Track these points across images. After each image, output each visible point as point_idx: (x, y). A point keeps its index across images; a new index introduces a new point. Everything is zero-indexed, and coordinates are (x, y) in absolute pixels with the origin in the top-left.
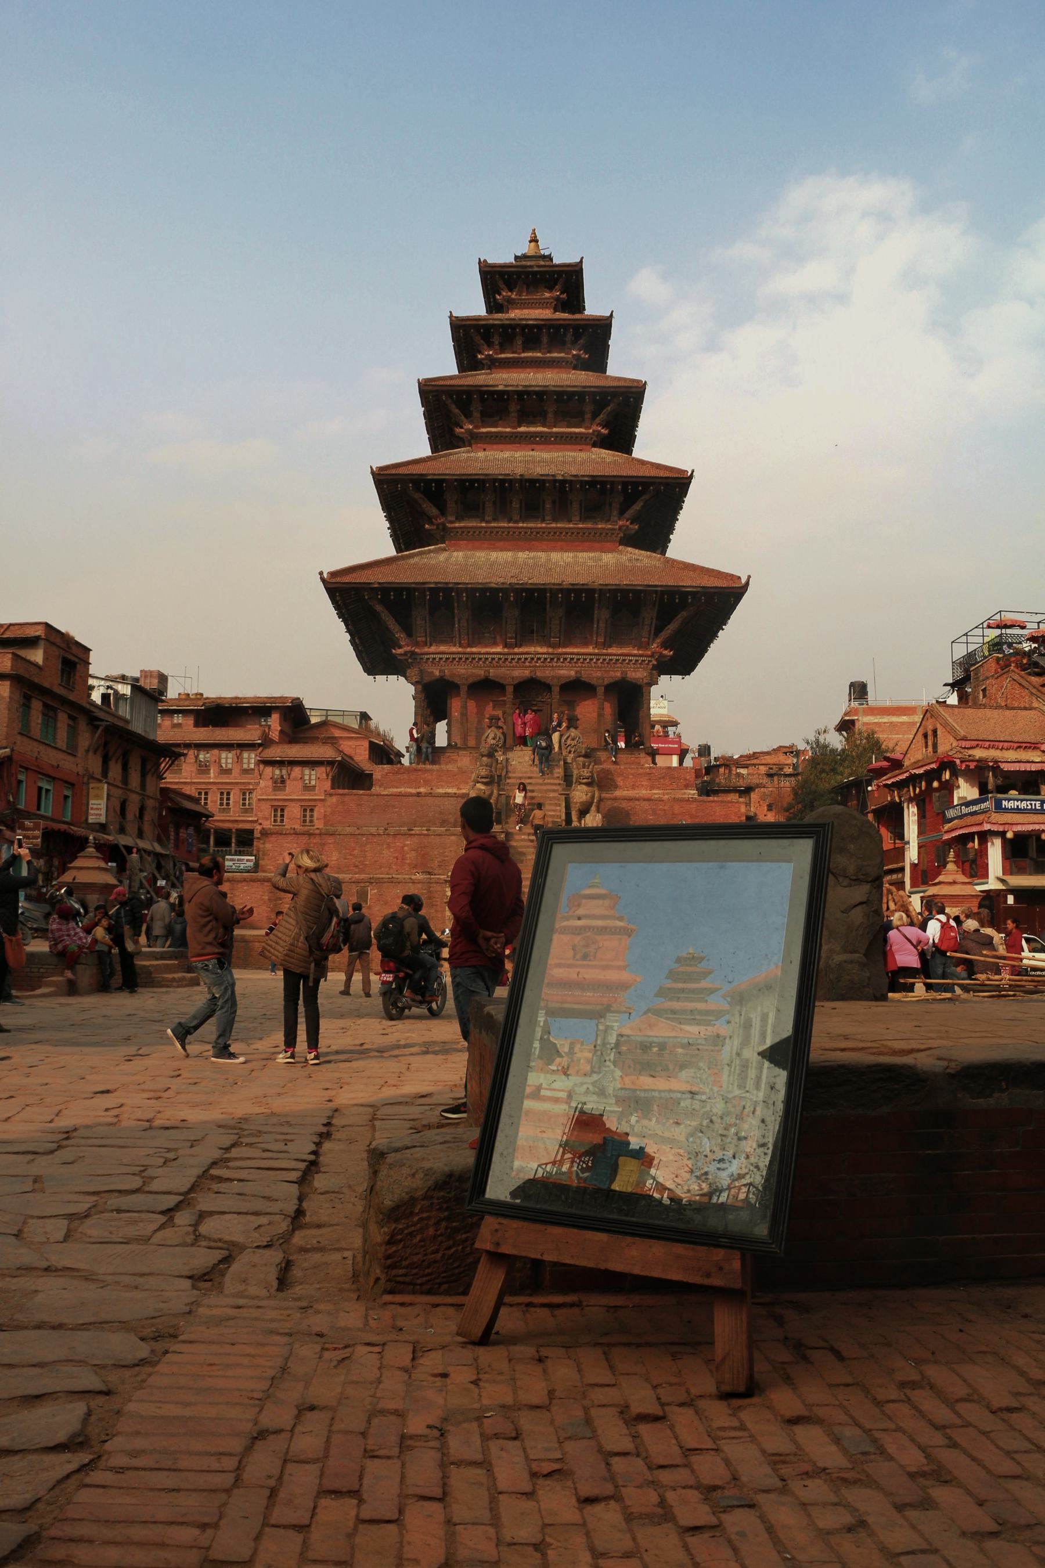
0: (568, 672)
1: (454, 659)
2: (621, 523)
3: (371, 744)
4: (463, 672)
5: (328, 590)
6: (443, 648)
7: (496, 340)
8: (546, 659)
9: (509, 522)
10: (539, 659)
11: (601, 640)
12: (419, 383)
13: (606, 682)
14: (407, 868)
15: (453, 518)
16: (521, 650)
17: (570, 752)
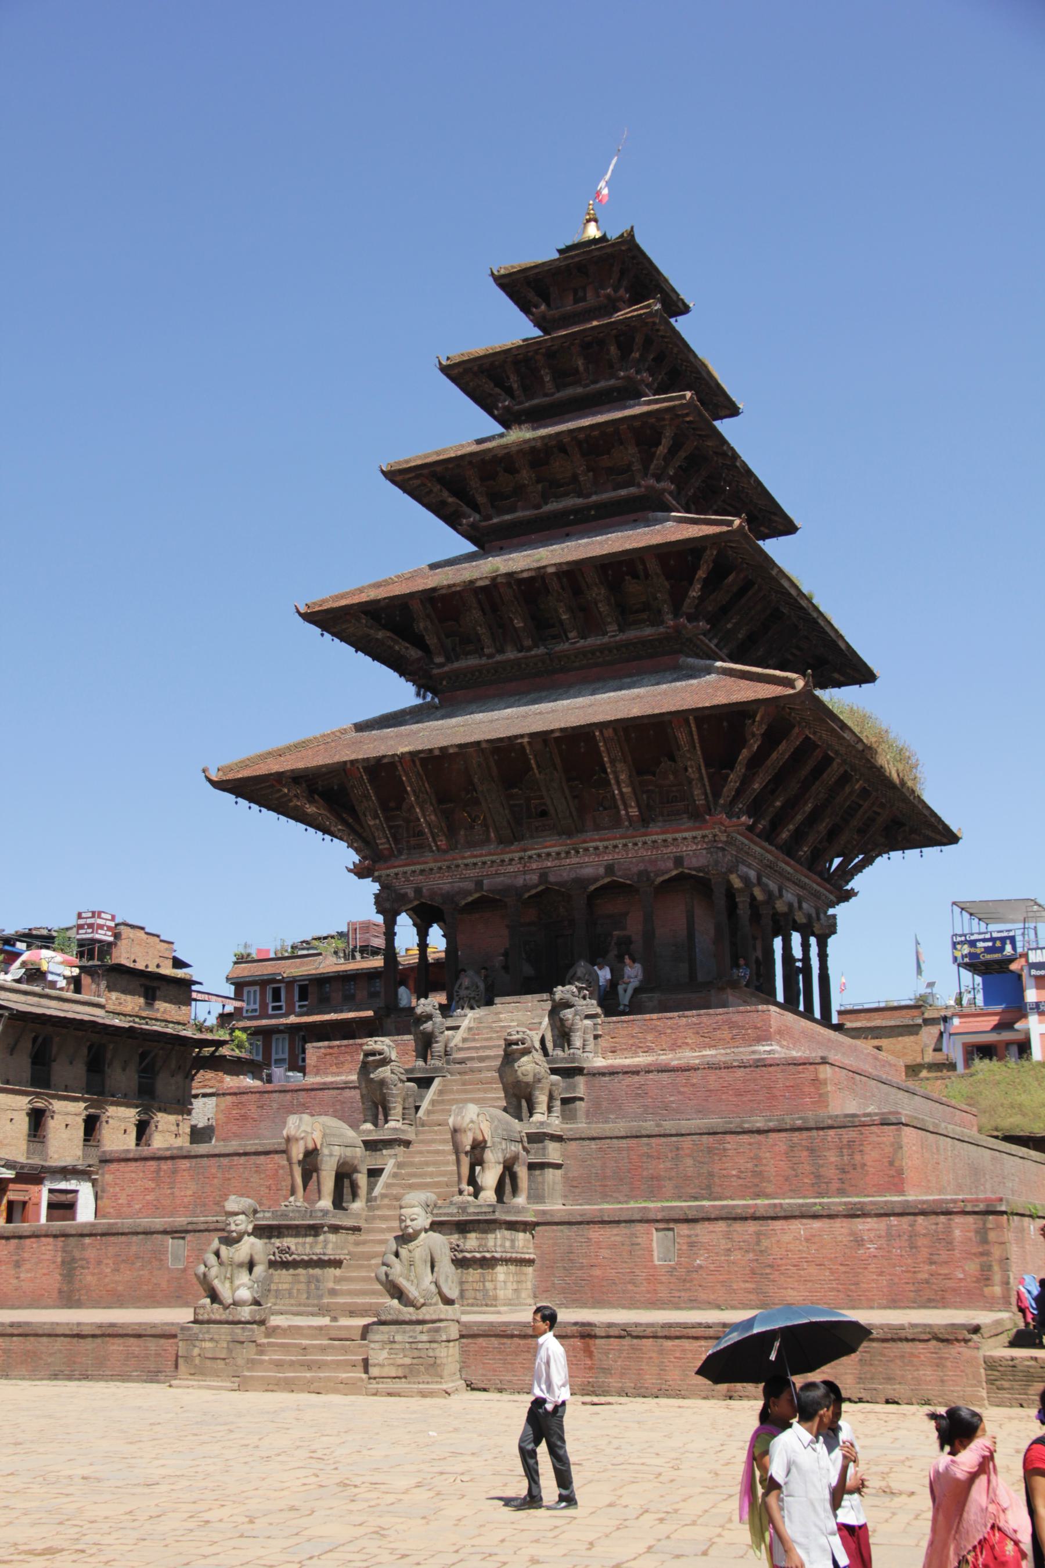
1: (431, 870)
8: (558, 854)
9: (520, 651)
10: (549, 854)
11: (634, 812)
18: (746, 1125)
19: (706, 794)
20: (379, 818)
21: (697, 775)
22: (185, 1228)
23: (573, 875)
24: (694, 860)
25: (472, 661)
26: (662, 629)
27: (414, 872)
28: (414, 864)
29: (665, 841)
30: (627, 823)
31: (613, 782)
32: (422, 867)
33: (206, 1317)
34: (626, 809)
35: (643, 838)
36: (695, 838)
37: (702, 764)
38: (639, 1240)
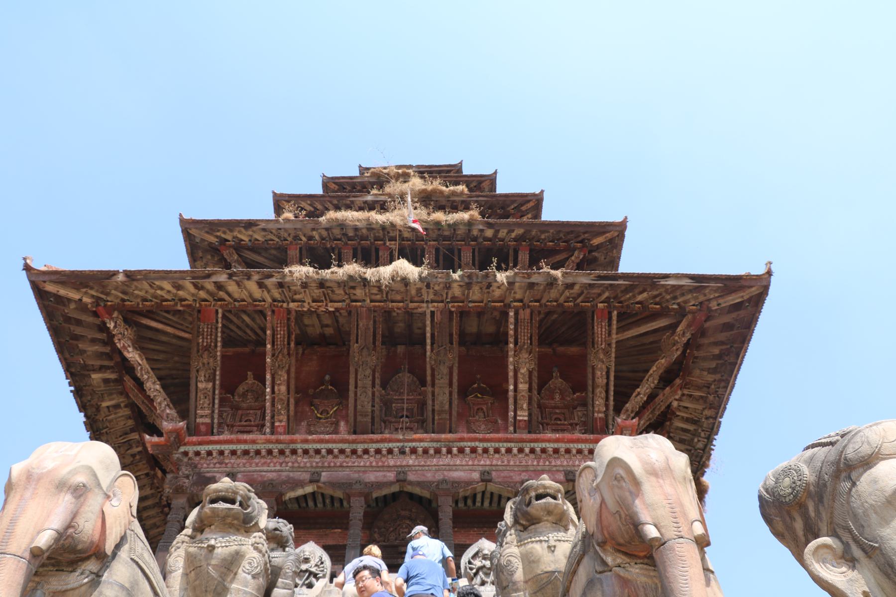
1: (258, 452)
5: (40, 294)
8: (426, 451)
10: (414, 451)
11: (523, 416)
12: (275, 194)
19: (607, 406)
21: (605, 381)
23: (439, 476)
27: (233, 453)
28: (239, 442)
29: (556, 451)
30: (511, 429)
31: (511, 374)
32: (246, 447)
34: (515, 411)
35: (532, 445)
37: (613, 369)
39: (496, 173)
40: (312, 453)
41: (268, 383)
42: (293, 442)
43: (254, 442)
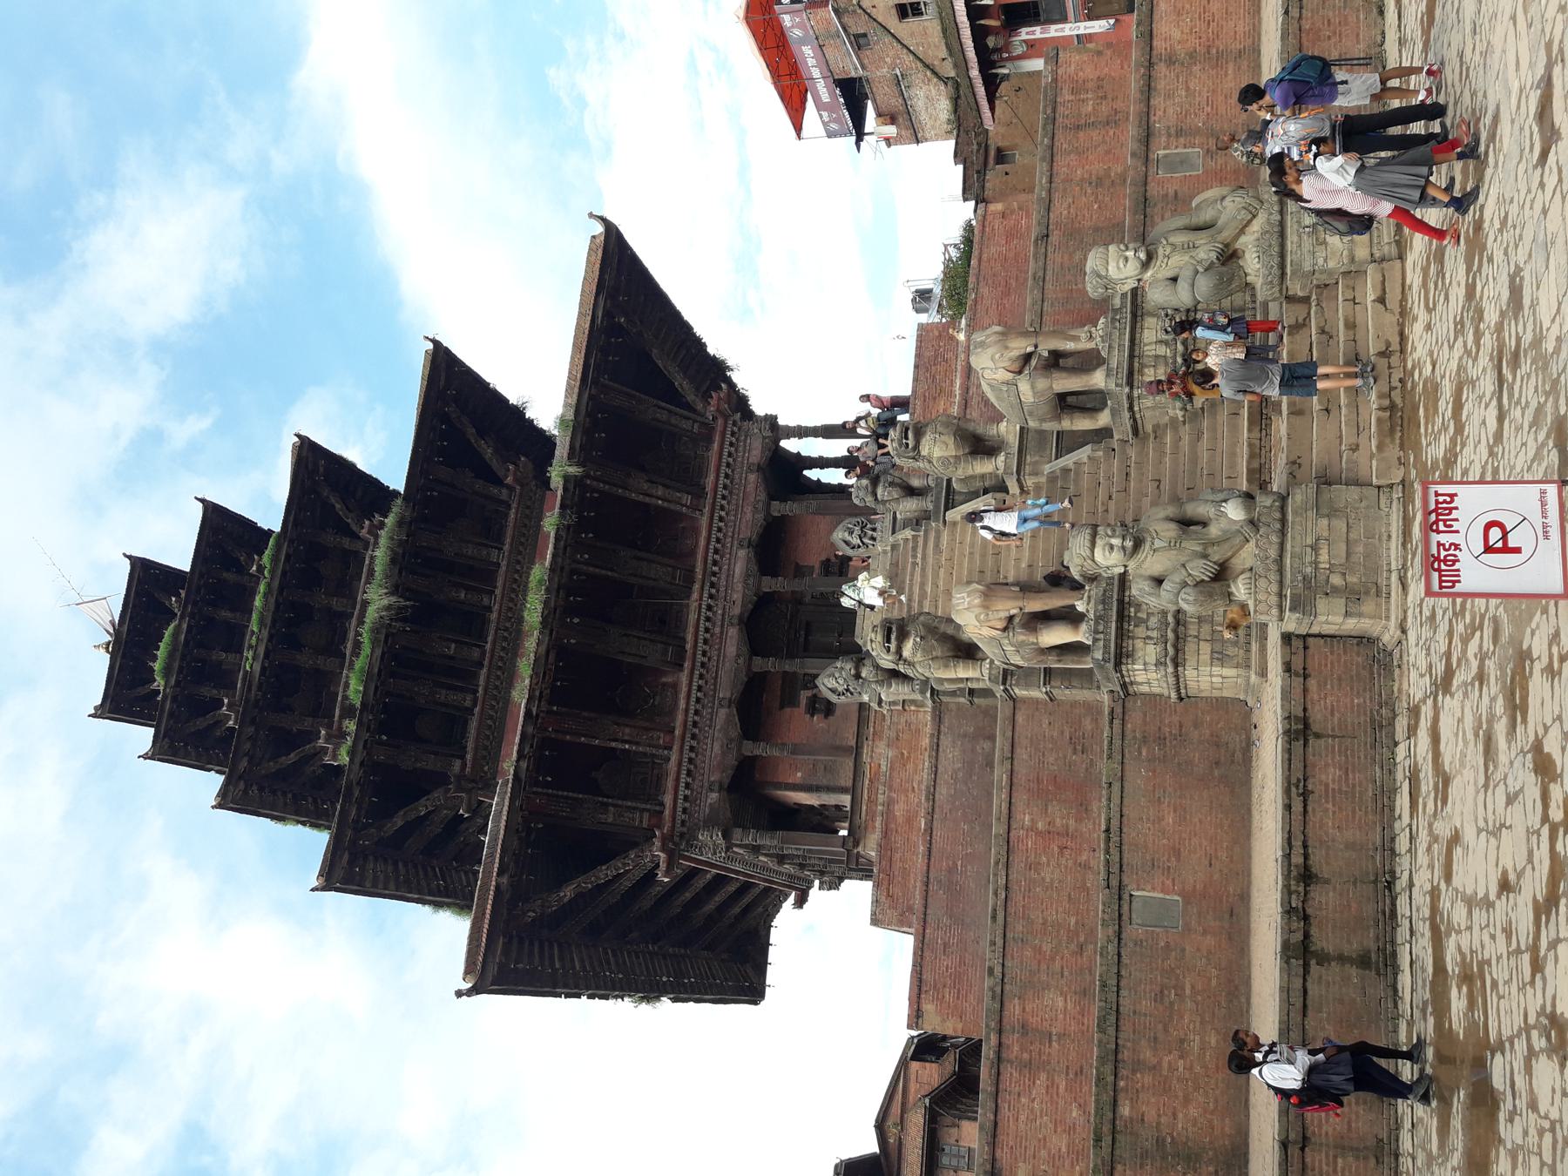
0: (740, 563)
1: (691, 761)
2: (509, 480)
3: (914, 1058)
4: (717, 746)
6: (670, 784)
7: (208, 692)
8: (711, 596)
10: (709, 608)
11: (687, 499)
12: (219, 806)
13: (763, 496)
14: (1086, 827)
15: (458, 763)
16: (689, 637)
17: (873, 539)
18: (1044, 194)
20: (607, 805)
22: (1115, 890)
23: (739, 587)
24: (754, 452)
25: (473, 725)
26: (514, 505)
27: (687, 786)
28: (677, 780)
29: (727, 476)
31: (647, 500)
33: (1274, 577)
36: (731, 444)
38: (1171, 192)
39: (202, 501)
40: (699, 707)
41: (620, 746)
42: (685, 722)
43: (680, 764)
